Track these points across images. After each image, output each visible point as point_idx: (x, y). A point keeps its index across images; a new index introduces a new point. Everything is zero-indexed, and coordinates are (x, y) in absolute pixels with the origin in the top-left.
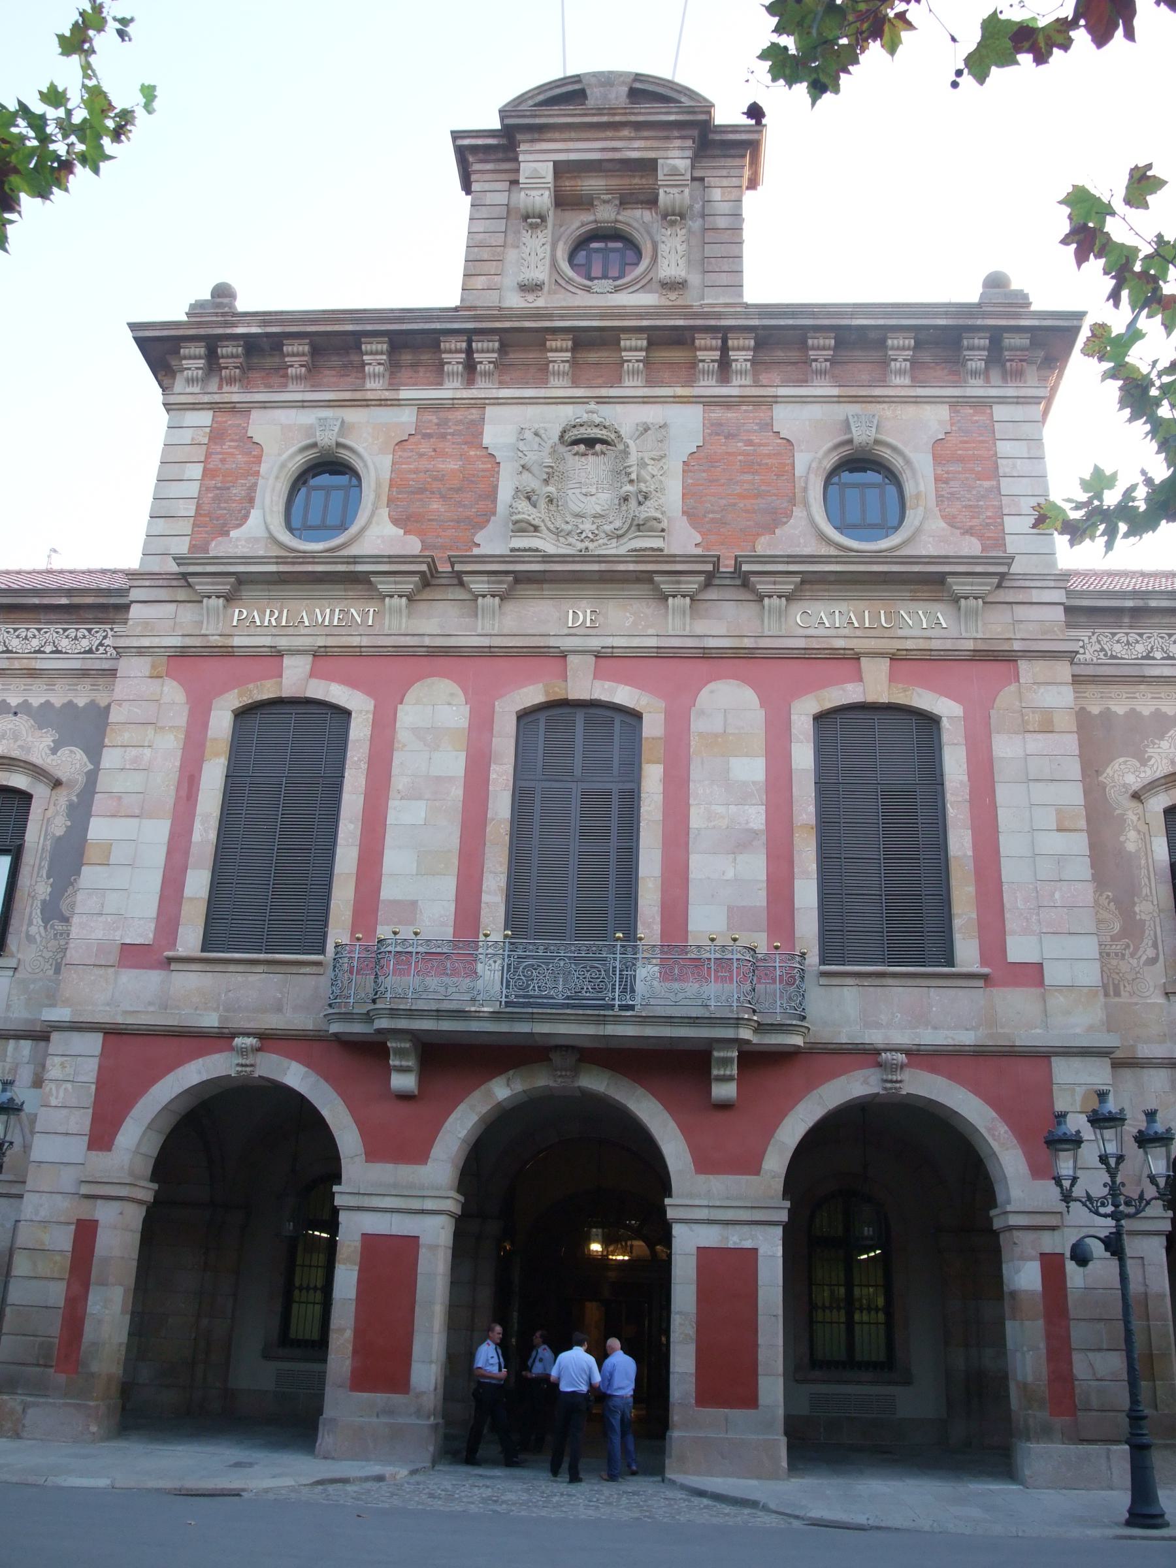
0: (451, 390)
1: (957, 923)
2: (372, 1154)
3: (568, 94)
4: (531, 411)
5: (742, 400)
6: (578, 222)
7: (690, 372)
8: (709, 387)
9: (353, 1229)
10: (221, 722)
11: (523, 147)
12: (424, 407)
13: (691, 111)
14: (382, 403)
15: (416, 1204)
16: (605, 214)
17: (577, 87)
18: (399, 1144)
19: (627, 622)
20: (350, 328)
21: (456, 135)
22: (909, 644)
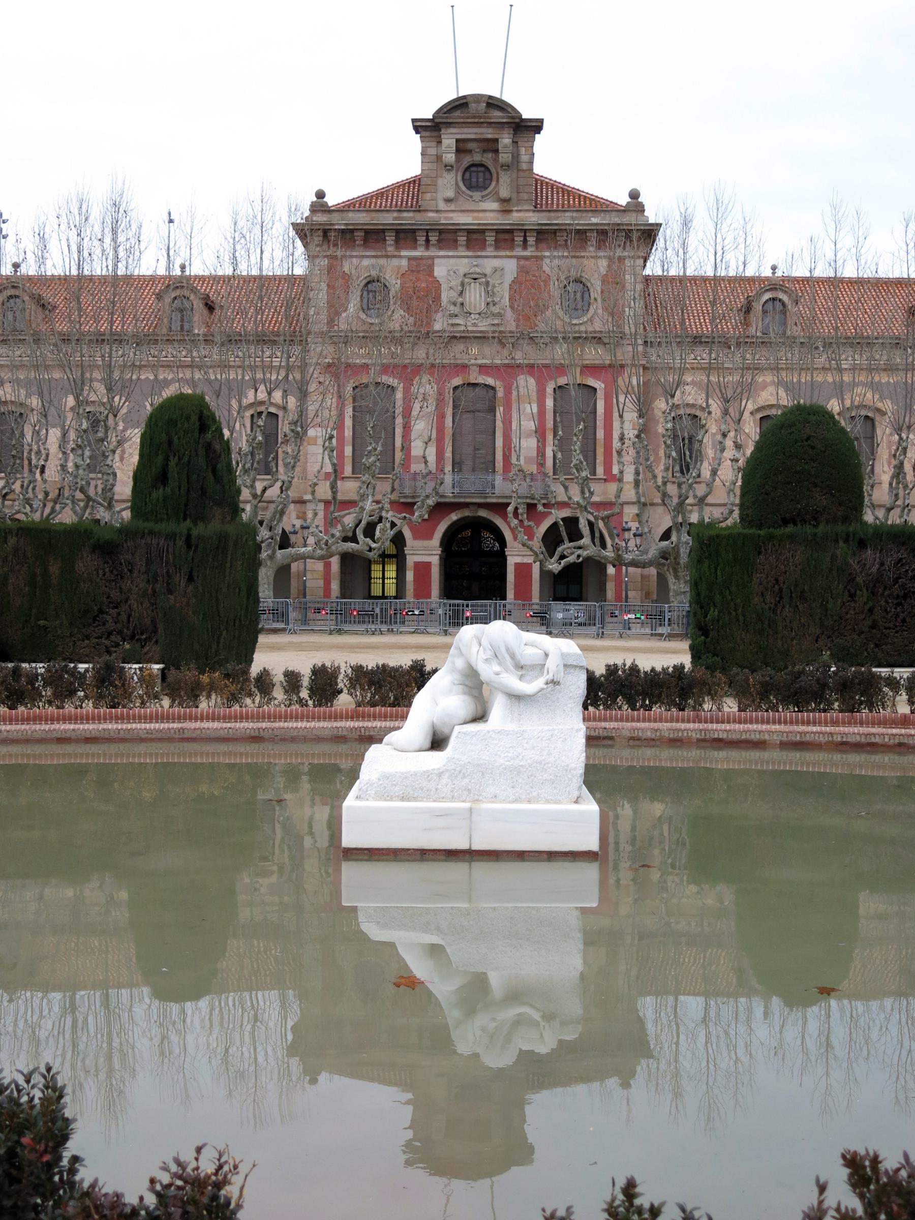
1: (597, 461)
2: (416, 537)
3: (460, 105)
4: (452, 261)
5: (531, 257)
6: (467, 160)
7: (511, 245)
9: (411, 560)
11: (443, 131)
12: (410, 259)
13: (512, 118)
14: (395, 256)
15: (430, 552)
16: (477, 158)
17: (464, 101)
18: (423, 532)
20: (381, 227)
21: (414, 121)
22: (587, 362)
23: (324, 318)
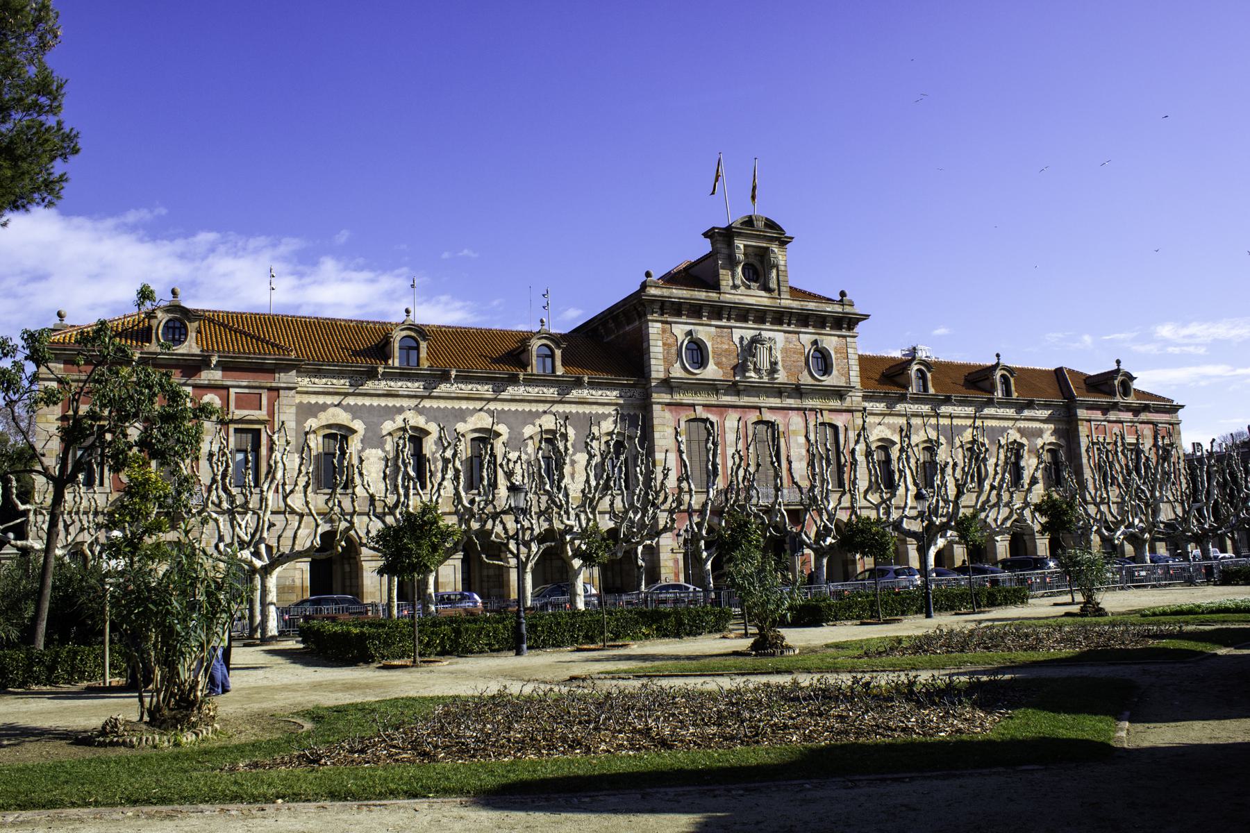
0: (724, 323)
7: (781, 324)
8: (785, 327)
10: (683, 424)
12: (717, 327)
19: (775, 402)
23: (662, 368)
